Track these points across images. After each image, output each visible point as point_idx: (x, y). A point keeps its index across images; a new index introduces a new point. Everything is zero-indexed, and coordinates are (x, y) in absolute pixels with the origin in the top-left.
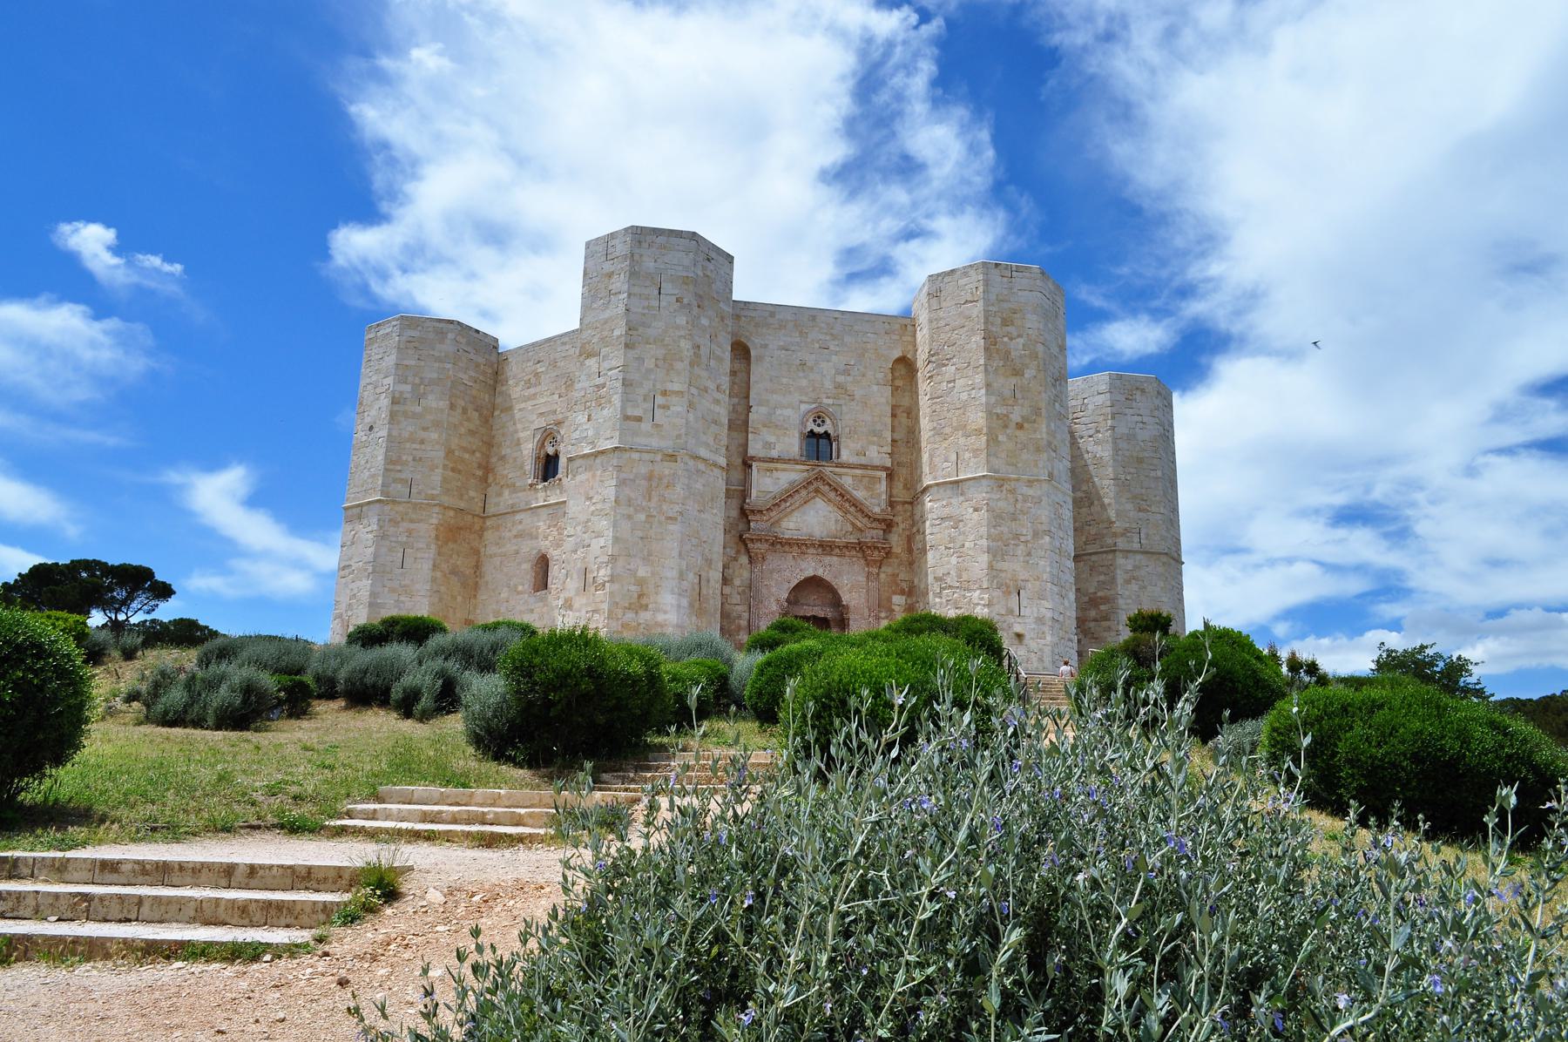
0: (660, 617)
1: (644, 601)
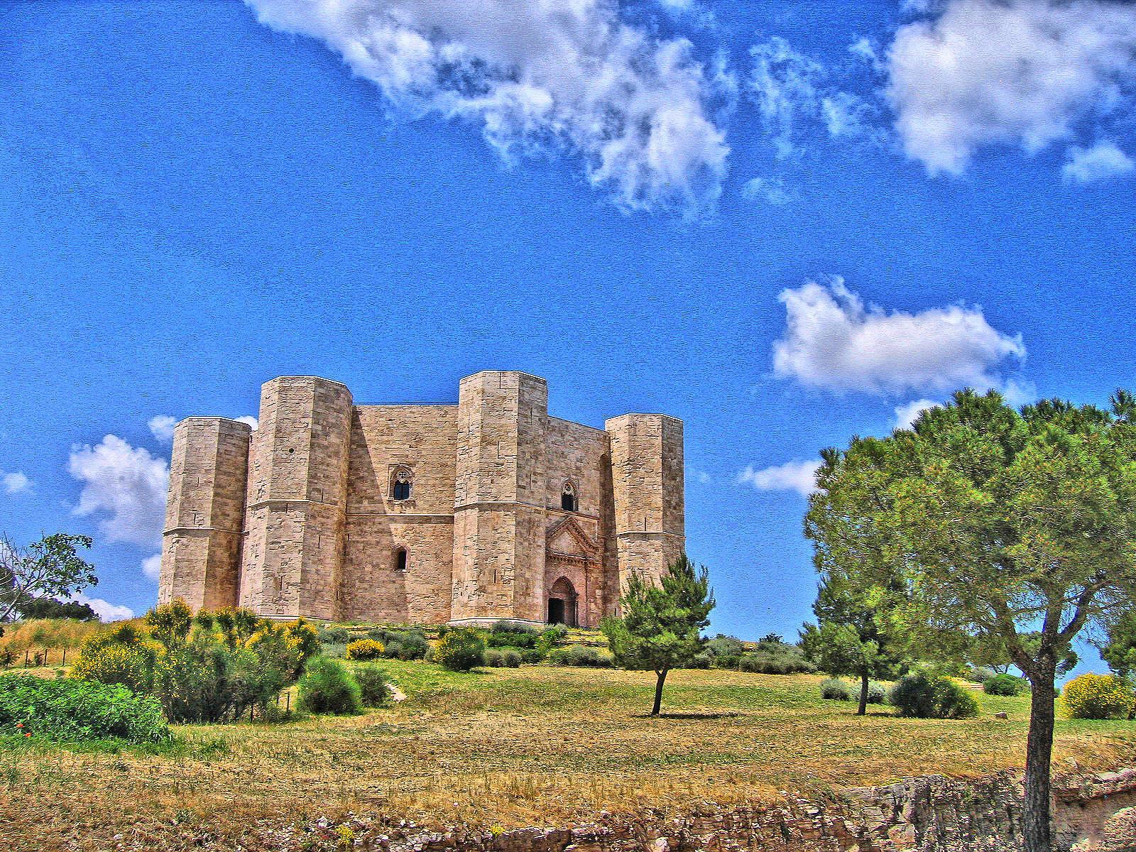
0: (535, 601)
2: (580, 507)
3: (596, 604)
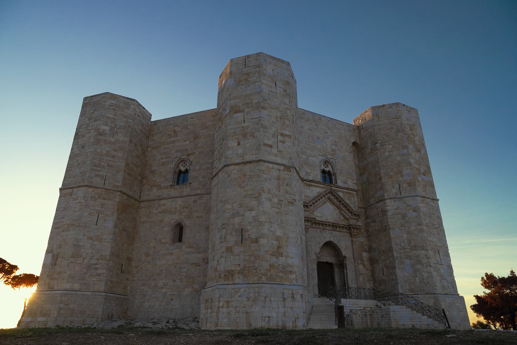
0: (290, 261)
1: (281, 250)
2: (338, 181)
3: (364, 266)
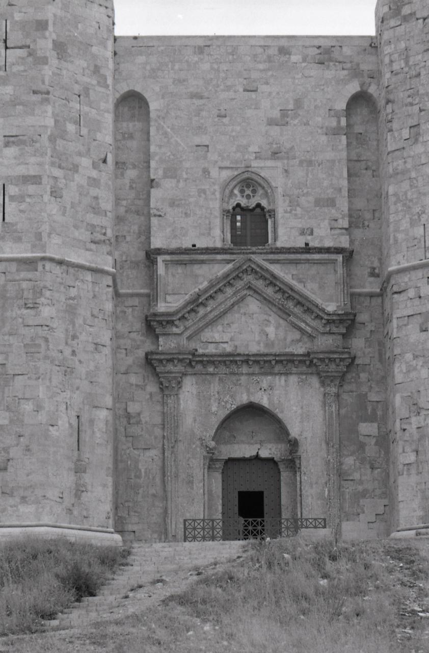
2: (281, 231)
